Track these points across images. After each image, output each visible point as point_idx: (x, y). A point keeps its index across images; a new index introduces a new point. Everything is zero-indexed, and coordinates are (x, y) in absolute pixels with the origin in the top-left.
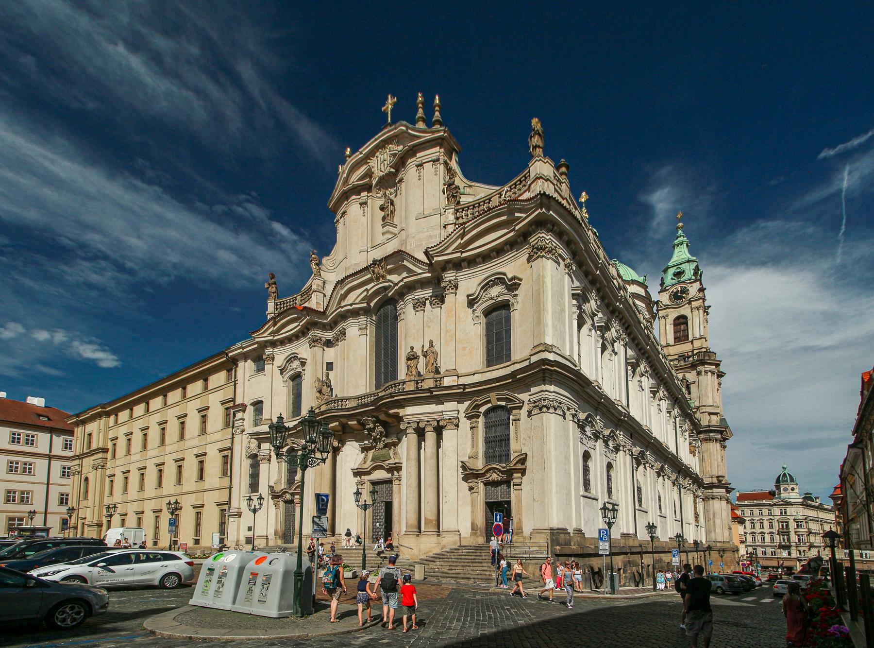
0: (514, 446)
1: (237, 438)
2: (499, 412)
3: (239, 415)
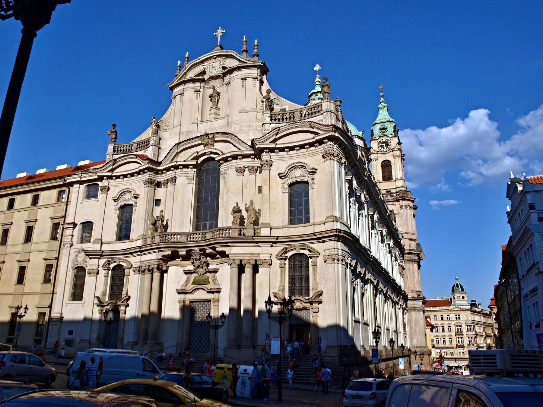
1: (65, 251)
2: (300, 258)
3: (68, 232)
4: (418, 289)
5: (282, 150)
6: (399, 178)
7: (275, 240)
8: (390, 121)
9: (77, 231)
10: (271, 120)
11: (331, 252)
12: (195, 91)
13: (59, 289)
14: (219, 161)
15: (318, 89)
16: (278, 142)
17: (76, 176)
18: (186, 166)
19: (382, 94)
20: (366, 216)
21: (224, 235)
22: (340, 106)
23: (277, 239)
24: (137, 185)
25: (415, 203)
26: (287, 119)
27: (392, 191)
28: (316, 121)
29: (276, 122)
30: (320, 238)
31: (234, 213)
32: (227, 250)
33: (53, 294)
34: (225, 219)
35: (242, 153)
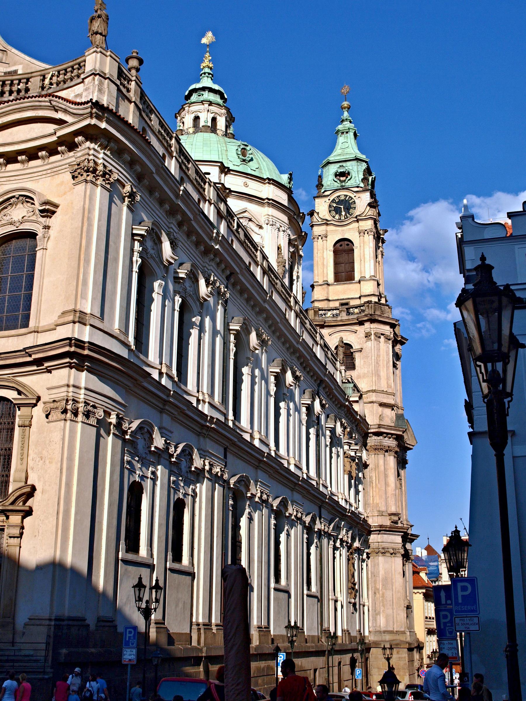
4: (393, 510)
6: (368, 277)
8: (357, 159)
11: (61, 393)
15: (206, 82)
19: (345, 104)
20: (215, 333)
22: (138, 70)
26: (11, 93)
27: (353, 303)
28: (71, 97)
30: (40, 361)
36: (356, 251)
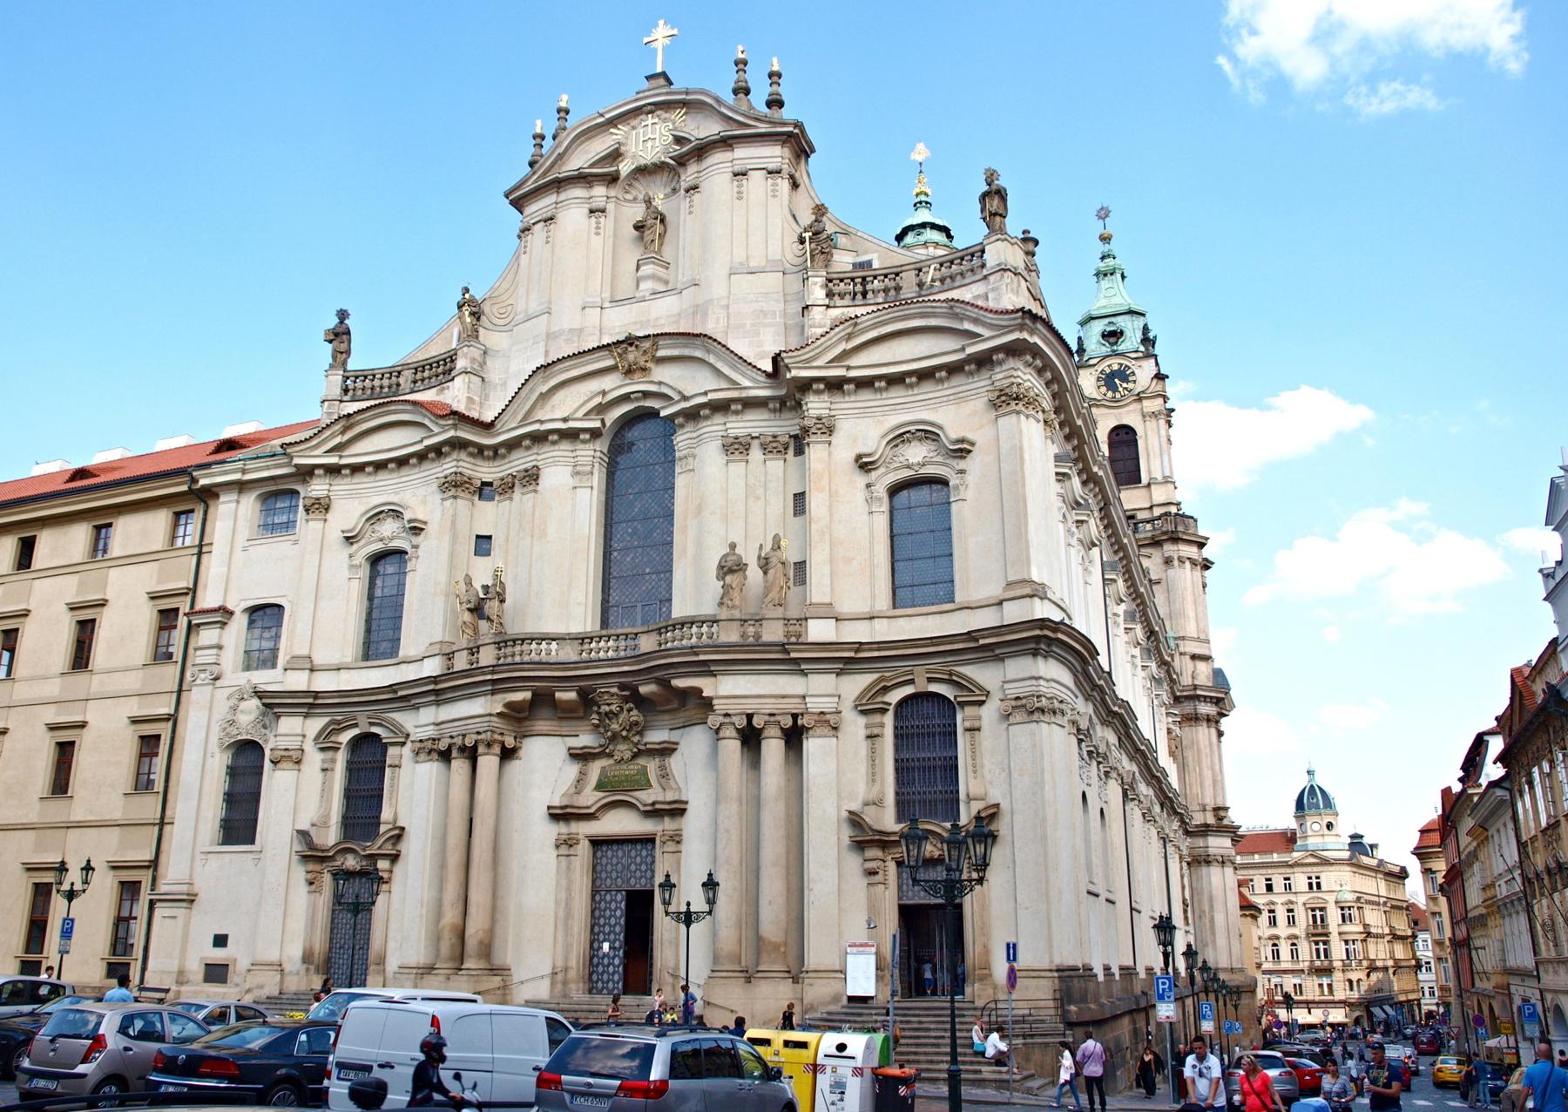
0: (967, 783)
1: (197, 697)
2: (926, 707)
3: (207, 636)
5: (865, 383)
7: (851, 654)
8: (1131, 312)
9: (236, 634)
10: (830, 295)
12: (592, 211)
13: (181, 809)
14: (672, 417)
16: (855, 361)
17: (227, 467)
18: (571, 435)
21: (694, 640)
23: (857, 651)
24: (417, 493)
25: (1206, 552)
27: (1141, 516)
29: (847, 301)
31: (725, 574)
32: (707, 686)
33: (162, 823)
34: (693, 591)
35: (744, 394)
36: (1140, 443)
